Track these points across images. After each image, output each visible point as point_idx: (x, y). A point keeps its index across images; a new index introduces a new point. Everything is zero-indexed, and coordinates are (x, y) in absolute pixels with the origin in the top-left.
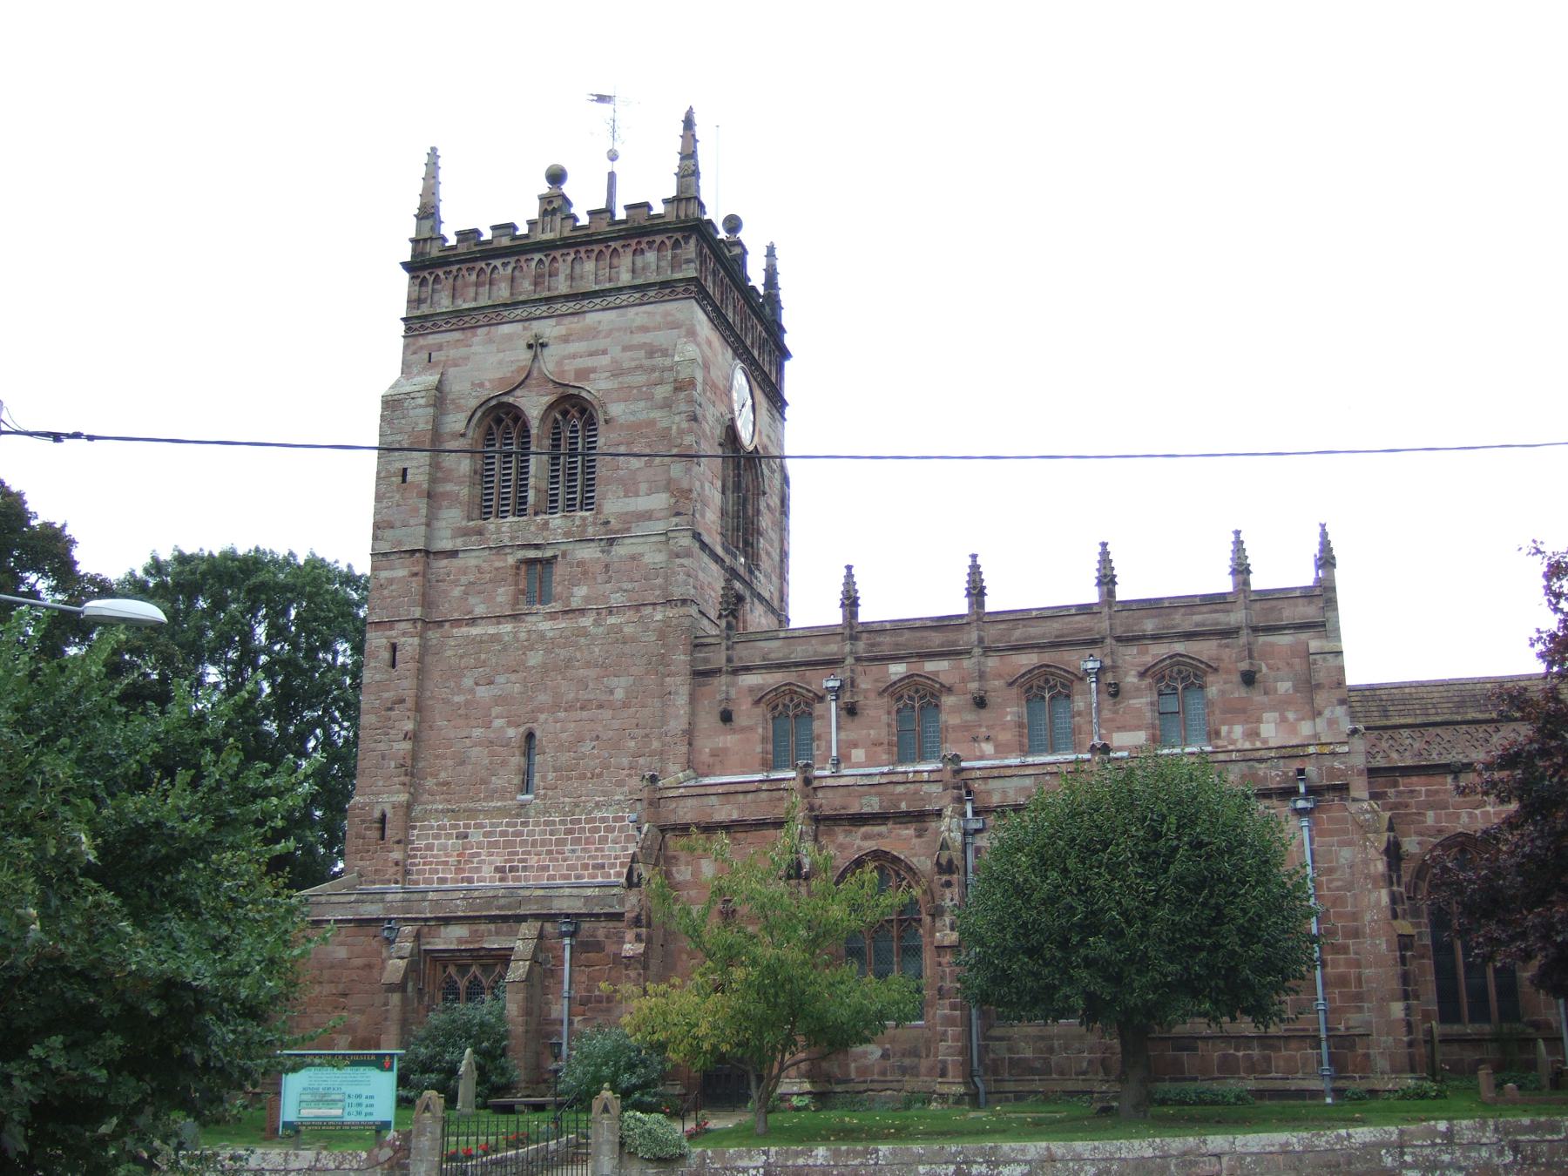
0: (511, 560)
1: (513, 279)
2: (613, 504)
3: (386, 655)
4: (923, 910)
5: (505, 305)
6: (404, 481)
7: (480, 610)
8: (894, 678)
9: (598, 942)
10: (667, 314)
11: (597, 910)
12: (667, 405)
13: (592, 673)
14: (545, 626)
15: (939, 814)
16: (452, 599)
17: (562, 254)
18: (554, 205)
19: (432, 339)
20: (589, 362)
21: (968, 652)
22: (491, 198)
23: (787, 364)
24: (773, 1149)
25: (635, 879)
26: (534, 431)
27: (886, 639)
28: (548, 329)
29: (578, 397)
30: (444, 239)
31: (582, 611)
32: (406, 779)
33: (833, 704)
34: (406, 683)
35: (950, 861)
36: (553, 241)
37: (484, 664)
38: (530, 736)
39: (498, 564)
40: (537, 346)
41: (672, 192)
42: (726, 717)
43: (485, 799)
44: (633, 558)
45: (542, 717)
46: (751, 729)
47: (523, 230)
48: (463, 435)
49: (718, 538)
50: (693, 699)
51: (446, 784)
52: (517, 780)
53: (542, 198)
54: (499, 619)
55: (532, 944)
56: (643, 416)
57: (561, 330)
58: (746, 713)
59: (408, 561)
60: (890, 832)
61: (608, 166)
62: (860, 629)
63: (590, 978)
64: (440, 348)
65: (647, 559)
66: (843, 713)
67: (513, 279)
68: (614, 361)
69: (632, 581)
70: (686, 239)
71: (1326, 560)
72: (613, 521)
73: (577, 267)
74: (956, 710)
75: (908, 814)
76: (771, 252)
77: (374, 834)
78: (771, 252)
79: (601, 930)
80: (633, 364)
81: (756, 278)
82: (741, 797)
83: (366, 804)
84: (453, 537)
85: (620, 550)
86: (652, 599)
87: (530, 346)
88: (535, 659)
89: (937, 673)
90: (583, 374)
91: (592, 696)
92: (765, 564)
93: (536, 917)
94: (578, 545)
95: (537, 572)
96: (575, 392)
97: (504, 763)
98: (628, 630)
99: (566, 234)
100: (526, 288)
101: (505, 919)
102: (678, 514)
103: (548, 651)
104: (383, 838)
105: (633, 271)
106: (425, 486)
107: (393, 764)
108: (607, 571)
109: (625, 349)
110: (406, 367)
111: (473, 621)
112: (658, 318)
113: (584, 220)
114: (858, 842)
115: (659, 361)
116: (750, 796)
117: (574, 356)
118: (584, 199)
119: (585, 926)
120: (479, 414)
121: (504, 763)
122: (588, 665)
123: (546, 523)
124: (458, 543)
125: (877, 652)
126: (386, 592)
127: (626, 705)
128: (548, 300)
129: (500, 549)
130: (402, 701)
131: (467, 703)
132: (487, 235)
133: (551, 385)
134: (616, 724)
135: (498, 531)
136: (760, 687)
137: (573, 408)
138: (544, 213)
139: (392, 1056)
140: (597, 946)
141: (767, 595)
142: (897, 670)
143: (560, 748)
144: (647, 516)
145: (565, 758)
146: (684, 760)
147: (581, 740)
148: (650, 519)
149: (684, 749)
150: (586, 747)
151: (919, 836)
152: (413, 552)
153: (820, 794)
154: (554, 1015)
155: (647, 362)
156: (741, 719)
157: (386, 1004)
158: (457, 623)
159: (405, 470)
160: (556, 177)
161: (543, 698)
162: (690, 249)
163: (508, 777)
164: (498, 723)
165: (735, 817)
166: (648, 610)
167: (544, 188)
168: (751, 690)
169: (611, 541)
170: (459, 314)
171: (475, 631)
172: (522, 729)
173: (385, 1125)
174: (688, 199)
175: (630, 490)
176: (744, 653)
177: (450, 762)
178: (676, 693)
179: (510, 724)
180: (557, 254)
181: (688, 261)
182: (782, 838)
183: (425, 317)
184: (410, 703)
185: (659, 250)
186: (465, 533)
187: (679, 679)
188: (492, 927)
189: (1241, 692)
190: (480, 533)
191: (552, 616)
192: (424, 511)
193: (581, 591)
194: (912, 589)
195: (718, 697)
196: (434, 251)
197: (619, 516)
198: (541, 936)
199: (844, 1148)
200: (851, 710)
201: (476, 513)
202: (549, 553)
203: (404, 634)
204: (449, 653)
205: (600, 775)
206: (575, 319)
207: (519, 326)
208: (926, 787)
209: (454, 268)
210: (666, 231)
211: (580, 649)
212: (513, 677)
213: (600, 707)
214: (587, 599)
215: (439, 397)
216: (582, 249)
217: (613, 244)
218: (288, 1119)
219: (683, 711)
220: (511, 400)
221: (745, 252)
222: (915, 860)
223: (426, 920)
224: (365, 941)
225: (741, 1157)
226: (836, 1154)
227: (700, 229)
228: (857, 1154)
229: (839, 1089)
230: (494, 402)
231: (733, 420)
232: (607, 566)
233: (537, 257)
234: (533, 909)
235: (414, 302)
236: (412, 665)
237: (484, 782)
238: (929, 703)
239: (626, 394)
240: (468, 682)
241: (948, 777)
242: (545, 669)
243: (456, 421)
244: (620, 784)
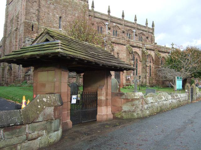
71: (153, 26)
130: (36, 2)
189: (146, 39)
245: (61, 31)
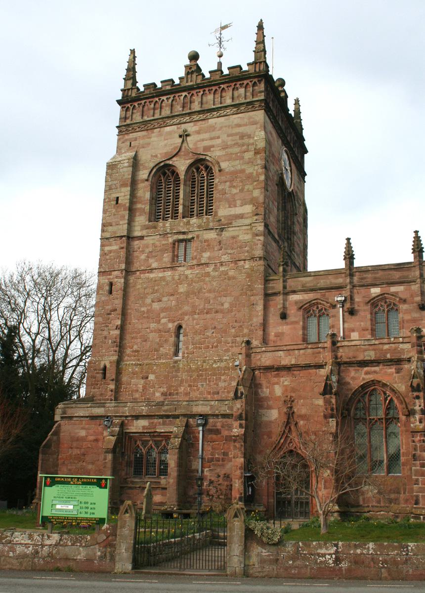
0: (170, 240)
1: (172, 106)
2: (223, 211)
3: (107, 288)
4: (400, 413)
5: (168, 117)
6: (117, 203)
7: (155, 265)
8: (374, 295)
9: (218, 430)
10: (250, 118)
11: (217, 412)
12: (251, 162)
13: (212, 295)
14: (188, 272)
15: (409, 360)
16: (140, 258)
17: (198, 88)
18: (193, 69)
19: (132, 136)
21: (414, 282)
22: (162, 67)
23: (306, 155)
24: (340, 543)
25: (239, 395)
26: (182, 177)
27: (369, 275)
28: (191, 128)
29: (204, 160)
30: (138, 89)
31: (207, 264)
32: (115, 348)
33: (341, 309)
34: (116, 302)
35: (418, 385)
36: (193, 85)
37: (157, 291)
38: (180, 327)
39: (164, 242)
40: (184, 136)
41: (252, 60)
42: (284, 316)
43: (157, 359)
44: (233, 237)
45: (186, 317)
46: (296, 323)
47: (177, 82)
48: (147, 180)
49: (276, 231)
50: (266, 308)
51: (137, 351)
52: (173, 350)
53: (186, 67)
54: (164, 269)
55: (182, 429)
56: (239, 167)
57: (196, 128)
58: (294, 315)
59: (119, 241)
60: (381, 370)
61: (218, 60)
62: (355, 270)
63: (213, 449)
64: (136, 139)
65: (241, 238)
66: (347, 314)
67: (172, 106)
68: (223, 142)
69: (232, 249)
70: (260, 81)
72: (223, 220)
73: (204, 98)
74: (407, 312)
75: (391, 360)
76: (297, 102)
77: (100, 376)
78: (297, 102)
79: (219, 423)
80: (233, 143)
81: (291, 112)
82: (296, 352)
83: (97, 361)
84: (141, 230)
85: (226, 234)
86: (243, 258)
87: (180, 136)
88: (182, 289)
89: (397, 293)
90: (208, 149)
91: (211, 307)
92: (297, 249)
93: (185, 415)
94: (205, 232)
96: (204, 157)
97: (166, 341)
98: (231, 273)
99: (199, 81)
100: (178, 109)
101: (168, 417)
102: (257, 215)
103: (189, 285)
104: (104, 378)
105: (233, 98)
106: (128, 205)
107: (110, 341)
108: (220, 244)
109: (228, 136)
110: (119, 149)
111: (152, 270)
112: (246, 120)
113: (207, 75)
114: (363, 376)
115: (246, 140)
116: (302, 351)
117: (203, 140)
118: (207, 66)
119: (211, 420)
120: (155, 170)
121: (166, 341)
122: (210, 291)
123: (189, 222)
124: (144, 233)
125: (364, 282)
126: (108, 257)
127: (230, 311)
128: (189, 114)
129: (165, 235)
130: (115, 310)
131: (148, 311)
132: (159, 85)
133: (191, 154)
134: (225, 321)
135: (164, 226)
136: (300, 301)
137: (201, 166)
138: (187, 74)
139: (106, 479)
140: (217, 432)
141: (298, 264)
142: (375, 291)
143: (195, 333)
144: (241, 216)
145: (197, 338)
146: (261, 338)
147: (206, 328)
148: (242, 218)
149: (261, 333)
150: (209, 334)
151: (397, 372)
152: (122, 237)
153: (341, 350)
154: (194, 467)
155: (240, 142)
156: (291, 318)
157: (105, 459)
158: (144, 271)
159: (118, 198)
160: (194, 57)
161: (186, 308)
162: (262, 86)
163: (168, 349)
164: (163, 321)
165: (293, 363)
167: (188, 62)
168: (296, 302)
169: (222, 230)
170: (145, 123)
171: (152, 275)
172: (176, 324)
173: (101, 521)
174: (260, 63)
175: (232, 204)
176: (293, 284)
177: (139, 340)
178: (257, 304)
179: (169, 321)
180: (194, 92)
181: (261, 92)
182: (324, 372)
183: (128, 125)
184: (119, 311)
185: (246, 88)
186: (148, 228)
187: (257, 298)
188: (161, 420)
190: (155, 227)
191: (192, 267)
192: (127, 217)
193: (206, 255)
194: (385, 246)
195: (279, 307)
196: (134, 94)
197: (225, 217)
198: (187, 425)
199: (385, 544)
200: (352, 312)
201: (153, 218)
202: (190, 236)
203: (117, 277)
204: (140, 286)
205: (217, 346)
206: (203, 122)
207: (175, 127)
208: (401, 346)
209: (143, 102)
210: (250, 78)
211: (206, 284)
212: (172, 298)
213: (217, 312)
214: (209, 258)
215: (135, 163)
216: (207, 89)
217: (222, 86)
218: (45, 514)
219: (261, 313)
220: (170, 162)
221: (286, 96)
222: (395, 385)
223: (126, 417)
224: (94, 427)
225: (321, 548)
226: (381, 547)
227: (266, 77)
228: (395, 548)
229: (353, 510)
230: (162, 164)
231: (282, 174)
232: (220, 242)
233: (184, 94)
234: (183, 411)
235: (123, 119)
236: (121, 293)
237: (157, 350)
238: (392, 308)
239: (230, 158)
240: (148, 301)
241: (414, 340)
242: (187, 294)
243: (143, 174)
244: (227, 351)
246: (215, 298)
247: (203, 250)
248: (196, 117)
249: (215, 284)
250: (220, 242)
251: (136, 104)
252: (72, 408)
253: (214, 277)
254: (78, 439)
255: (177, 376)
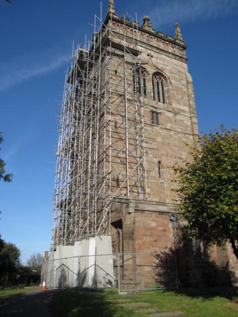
2: (175, 105)
10: (182, 65)
13: (176, 149)
20: (164, 67)
28: (152, 53)
36: (152, 33)
38: (159, 162)
44: (182, 121)
45: (164, 157)
56: (180, 86)
72: (176, 109)
85: (179, 117)
95: (155, 115)
97: (154, 169)
103: (163, 139)
109: (173, 68)
112: (180, 65)
122: (174, 146)
144: (184, 111)
161: (162, 152)
163: (154, 173)
166: (187, 135)
169: (176, 114)
172: (158, 160)
175: (179, 103)
179: (154, 157)
202: (159, 111)
207: (144, 49)
211: (172, 141)
214: (171, 127)
233: (147, 35)
239: (175, 79)
242: (163, 144)
245: (162, 183)
246: (177, 151)
247: (167, 122)
248: (154, 49)
249: (176, 142)
250: (175, 120)
251: (119, 24)
252: (142, 203)
253: (175, 139)
254: (151, 229)
255: (163, 192)
